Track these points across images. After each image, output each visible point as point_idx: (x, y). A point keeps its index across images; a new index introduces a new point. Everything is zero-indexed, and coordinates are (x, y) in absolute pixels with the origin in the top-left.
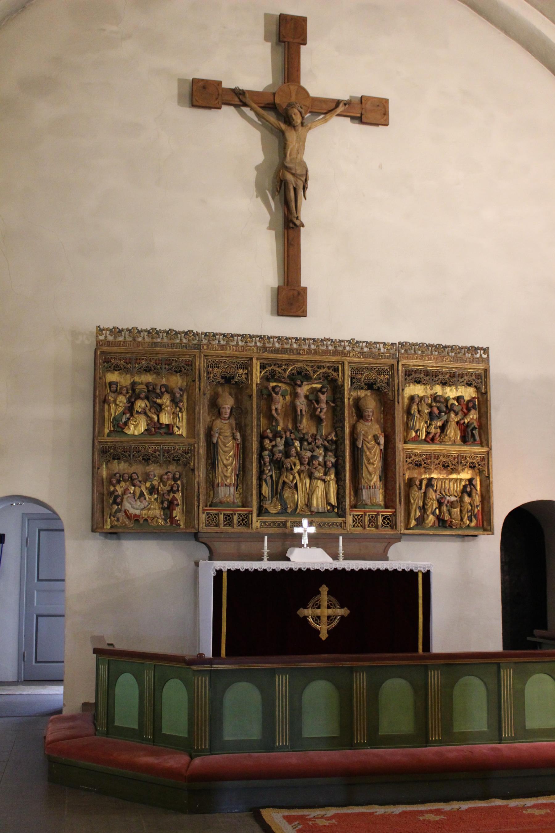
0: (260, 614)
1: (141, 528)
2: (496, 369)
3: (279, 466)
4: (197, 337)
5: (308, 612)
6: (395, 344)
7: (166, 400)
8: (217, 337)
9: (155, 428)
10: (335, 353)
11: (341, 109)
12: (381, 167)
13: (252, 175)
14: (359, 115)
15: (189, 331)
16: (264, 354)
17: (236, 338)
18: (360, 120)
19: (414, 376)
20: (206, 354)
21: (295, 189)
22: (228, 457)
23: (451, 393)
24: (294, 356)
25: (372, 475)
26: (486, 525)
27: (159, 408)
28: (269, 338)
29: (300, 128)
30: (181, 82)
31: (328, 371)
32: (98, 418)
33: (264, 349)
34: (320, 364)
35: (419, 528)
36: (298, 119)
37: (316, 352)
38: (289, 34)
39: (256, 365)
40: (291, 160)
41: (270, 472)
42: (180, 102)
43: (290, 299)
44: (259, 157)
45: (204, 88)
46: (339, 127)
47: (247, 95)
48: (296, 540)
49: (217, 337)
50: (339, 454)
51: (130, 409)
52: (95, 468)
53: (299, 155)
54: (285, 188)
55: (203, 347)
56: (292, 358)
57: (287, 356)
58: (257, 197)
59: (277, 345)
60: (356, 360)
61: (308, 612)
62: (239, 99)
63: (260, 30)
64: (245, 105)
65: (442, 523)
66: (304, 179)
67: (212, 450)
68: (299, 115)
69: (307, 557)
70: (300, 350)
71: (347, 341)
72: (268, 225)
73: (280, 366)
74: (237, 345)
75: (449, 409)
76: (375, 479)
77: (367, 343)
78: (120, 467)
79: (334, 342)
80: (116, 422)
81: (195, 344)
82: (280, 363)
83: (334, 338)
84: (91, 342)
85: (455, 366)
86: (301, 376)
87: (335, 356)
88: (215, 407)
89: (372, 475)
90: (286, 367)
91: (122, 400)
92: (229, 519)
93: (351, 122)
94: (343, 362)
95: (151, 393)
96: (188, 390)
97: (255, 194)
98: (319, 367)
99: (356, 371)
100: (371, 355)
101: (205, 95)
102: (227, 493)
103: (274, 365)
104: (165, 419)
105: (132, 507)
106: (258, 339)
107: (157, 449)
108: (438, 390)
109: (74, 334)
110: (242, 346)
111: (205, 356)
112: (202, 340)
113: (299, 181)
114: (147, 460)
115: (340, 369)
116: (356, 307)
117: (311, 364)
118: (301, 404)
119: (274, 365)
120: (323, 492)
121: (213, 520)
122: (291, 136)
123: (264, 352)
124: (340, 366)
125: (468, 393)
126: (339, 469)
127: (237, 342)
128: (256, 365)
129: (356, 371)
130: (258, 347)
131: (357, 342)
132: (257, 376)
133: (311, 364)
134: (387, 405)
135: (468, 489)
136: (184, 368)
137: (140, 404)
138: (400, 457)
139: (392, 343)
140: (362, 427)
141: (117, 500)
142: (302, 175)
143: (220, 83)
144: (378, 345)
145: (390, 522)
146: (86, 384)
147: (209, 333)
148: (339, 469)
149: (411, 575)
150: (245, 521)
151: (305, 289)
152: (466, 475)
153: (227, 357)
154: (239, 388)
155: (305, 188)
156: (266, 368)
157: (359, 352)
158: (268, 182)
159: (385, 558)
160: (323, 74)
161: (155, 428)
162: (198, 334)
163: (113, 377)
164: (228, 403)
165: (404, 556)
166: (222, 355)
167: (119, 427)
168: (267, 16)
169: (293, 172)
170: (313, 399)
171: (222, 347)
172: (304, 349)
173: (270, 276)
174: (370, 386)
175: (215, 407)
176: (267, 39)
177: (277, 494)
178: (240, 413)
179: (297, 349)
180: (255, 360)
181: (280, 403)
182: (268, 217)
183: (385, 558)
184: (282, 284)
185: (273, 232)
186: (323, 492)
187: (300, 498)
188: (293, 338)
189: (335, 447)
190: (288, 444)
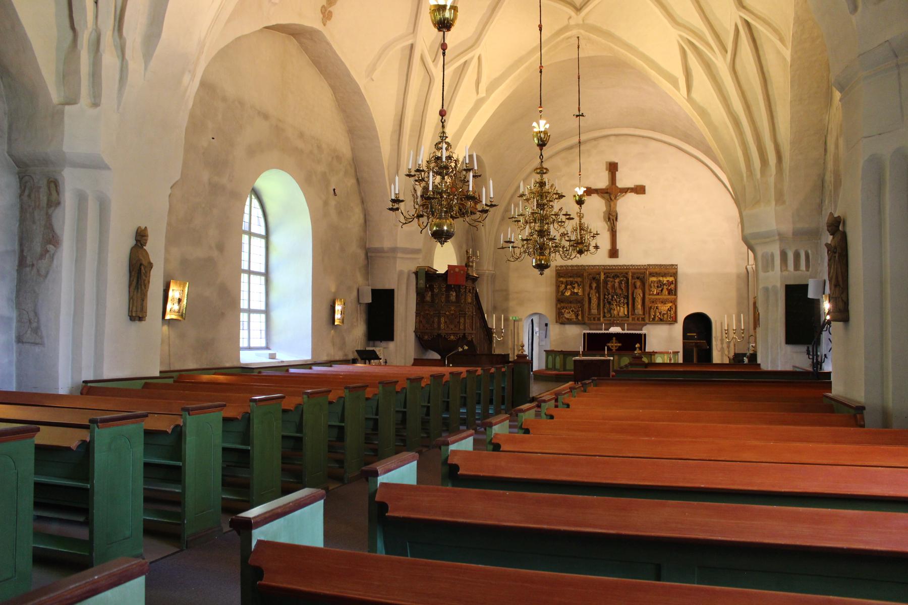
0: (594, 343)
1: (569, 322)
2: (680, 271)
3: (610, 303)
7: (576, 285)
9: (573, 293)
19: (652, 275)
22: (594, 301)
23: (665, 280)
25: (639, 306)
26: (675, 320)
27: (574, 288)
38: (613, 168)
39: (602, 274)
44: (604, 209)
46: (631, 196)
51: (566, 288)
54: (611, 218)
62: (597, 191)
63: (605, 167)
65: (661, 320)
67: (590, 299)
76: (640, 306)
85: (666, 271)
86: (616, 276)
88: (591, 287)
89: (639, 306)
95: (572, 283)
96: (582, 282)
99: (633, 274)
102: (594, 311)
104: (576, 291)
105: (567, 316)
107: (576, 300)
108: (661, 279)
114: (571, 302)
116: (635, 254)
118: (617, 285)
120: (623, 311)
121: (589, 319)
122: (612, 204)
125: (671, 279)
128: (602, 274)
129: (633, 274)
132: (602, 277)
134: (643, 284)
138: (647, 300)
141: (563, 314)
145: (643, 319)
146: (554, 280)
149: (640, 335)
150: (599, 319)
154: (598, 281)
160: (623, 181)
161: (573, 293)
163: (561, 279)
164: (594, 285)
167: (563, 293)
170: (620, 283)
174: (638, 278)
175: (591, 287)
178: (598, 288)
181: (609, 286)
187: (616, 312)
189: (627, 297)
190: (613, 297)
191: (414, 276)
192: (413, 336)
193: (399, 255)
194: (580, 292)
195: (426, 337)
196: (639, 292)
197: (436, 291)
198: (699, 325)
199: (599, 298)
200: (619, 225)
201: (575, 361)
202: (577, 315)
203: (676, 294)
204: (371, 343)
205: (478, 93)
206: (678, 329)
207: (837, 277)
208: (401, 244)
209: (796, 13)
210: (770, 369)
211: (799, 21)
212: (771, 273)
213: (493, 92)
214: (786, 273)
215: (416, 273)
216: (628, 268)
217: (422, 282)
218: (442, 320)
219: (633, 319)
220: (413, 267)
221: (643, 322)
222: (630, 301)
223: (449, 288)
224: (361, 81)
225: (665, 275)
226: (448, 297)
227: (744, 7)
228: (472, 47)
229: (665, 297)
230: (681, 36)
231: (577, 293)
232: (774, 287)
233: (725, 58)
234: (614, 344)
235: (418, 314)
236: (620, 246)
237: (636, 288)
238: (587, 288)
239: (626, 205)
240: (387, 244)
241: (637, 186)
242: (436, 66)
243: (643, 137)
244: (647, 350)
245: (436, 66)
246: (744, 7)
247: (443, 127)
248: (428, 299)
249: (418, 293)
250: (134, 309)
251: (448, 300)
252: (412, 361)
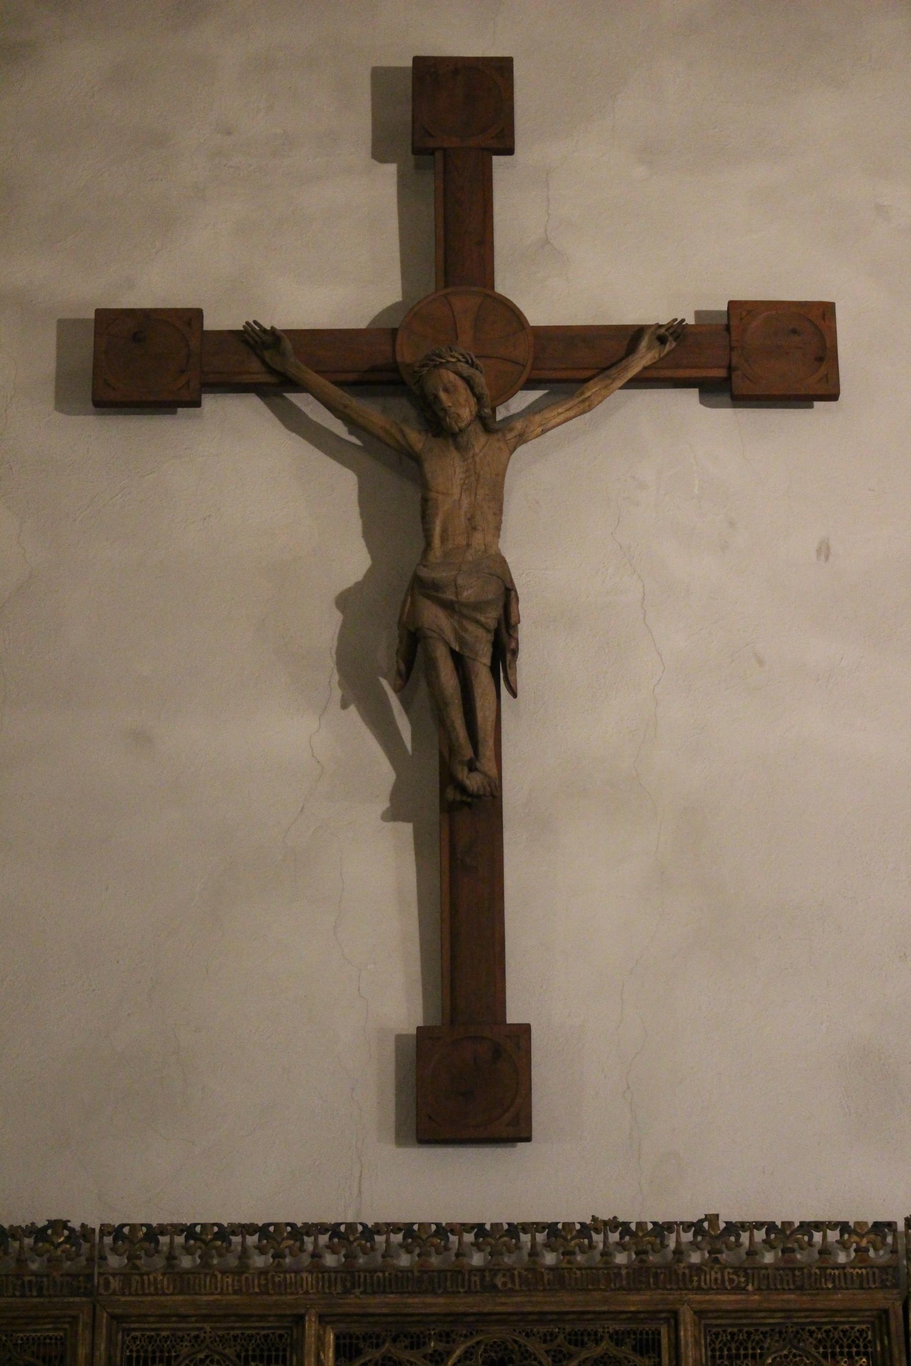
4: (86, 1246)
6: (891, 1225)
8: (164, 1240)
10: (640, 1276)
11: (645, 357)
12: (824, 551)
13: (324, 628)
14: (722, 373)
15: (52, 1224)
16: (351, 1299)
17: (236, 1239)
20: (118, 1311)
21: (459, 661)
24: (470, 1300)
28: (370, 1232)
29: (479, 442)
30: (66, 327)
31: (614, 1351)
33: (349, 1276)
34: (579, 1327)
36: (462, 408)
37: (559, 1278)
38: (452, 126)
40: (446, 554)
42: (65, 401)
43: (467, 1072)
44: (352, 561)
45: (137, 338)
47: (288, 345)
49: (164, 1240)
53: (478, 539)
54: (437, 660)
55: (107, 1284)
56: (461, 1309)
57: (441, 1300)
58: (344, 706)
59: (404, 1260)
60: (726, 1300)
63: (360, 121)
64: (297, 386)
66: (491, 617)
68: (463, 392)
70: (494, 1272)
71: (687, 1226)
72: (384, 804)
73: (416, 1343)
74: (243, 1267)
77: (771, 1227)
79: (633, 1234)
81: (75, 1276)
82: (414, 1330)
83: (631, 1215)
87: (638, 1290)
90: (441, 1346)
93: (702, 402)
94: (675, 1314)
97: (338, 693)
98: (577, 1339)
100: (790, 1275)
101: (147, 364)
103: (394, 1340)
106: (324, 1239)
110: (263, 1272)
111: (113, 1317)
112: (103, 1258)
113: (471, 627)
115: (664, 1341)
117: (543, 1329)
119: (394, 1340)
122: (448, 473)
123: (347, 1291)
124: (664, 1331)
127: (244, 1253)
130: (324, 1270)
131: (733, 1228)
133: (543, 1329)
139: (876, 1225)
142: (478, 606)
143: (198, 314)
144: (817, 1237)
147: (133, 1227)
151: (524, 1030)
153: (205, 1318)
155: (503, 651)
156: (359, 1352)
157: (736, 1270)
158: (384, 648)
160: (580, 245)
162: (86, 1232)
166: (182, 1311)
168: (380, 76)
169: (449, 596)
171: (183, 1281)
172: (510, 1269)
176: (380, 153)
179: (480, 1270)
180: (311, 1327)
182: (384, 773)
184: (436, 1021)
185: (407, 829)
188: (466, 1227)
200: (540, 746)
236: (538, 986)
239: (606, 521)
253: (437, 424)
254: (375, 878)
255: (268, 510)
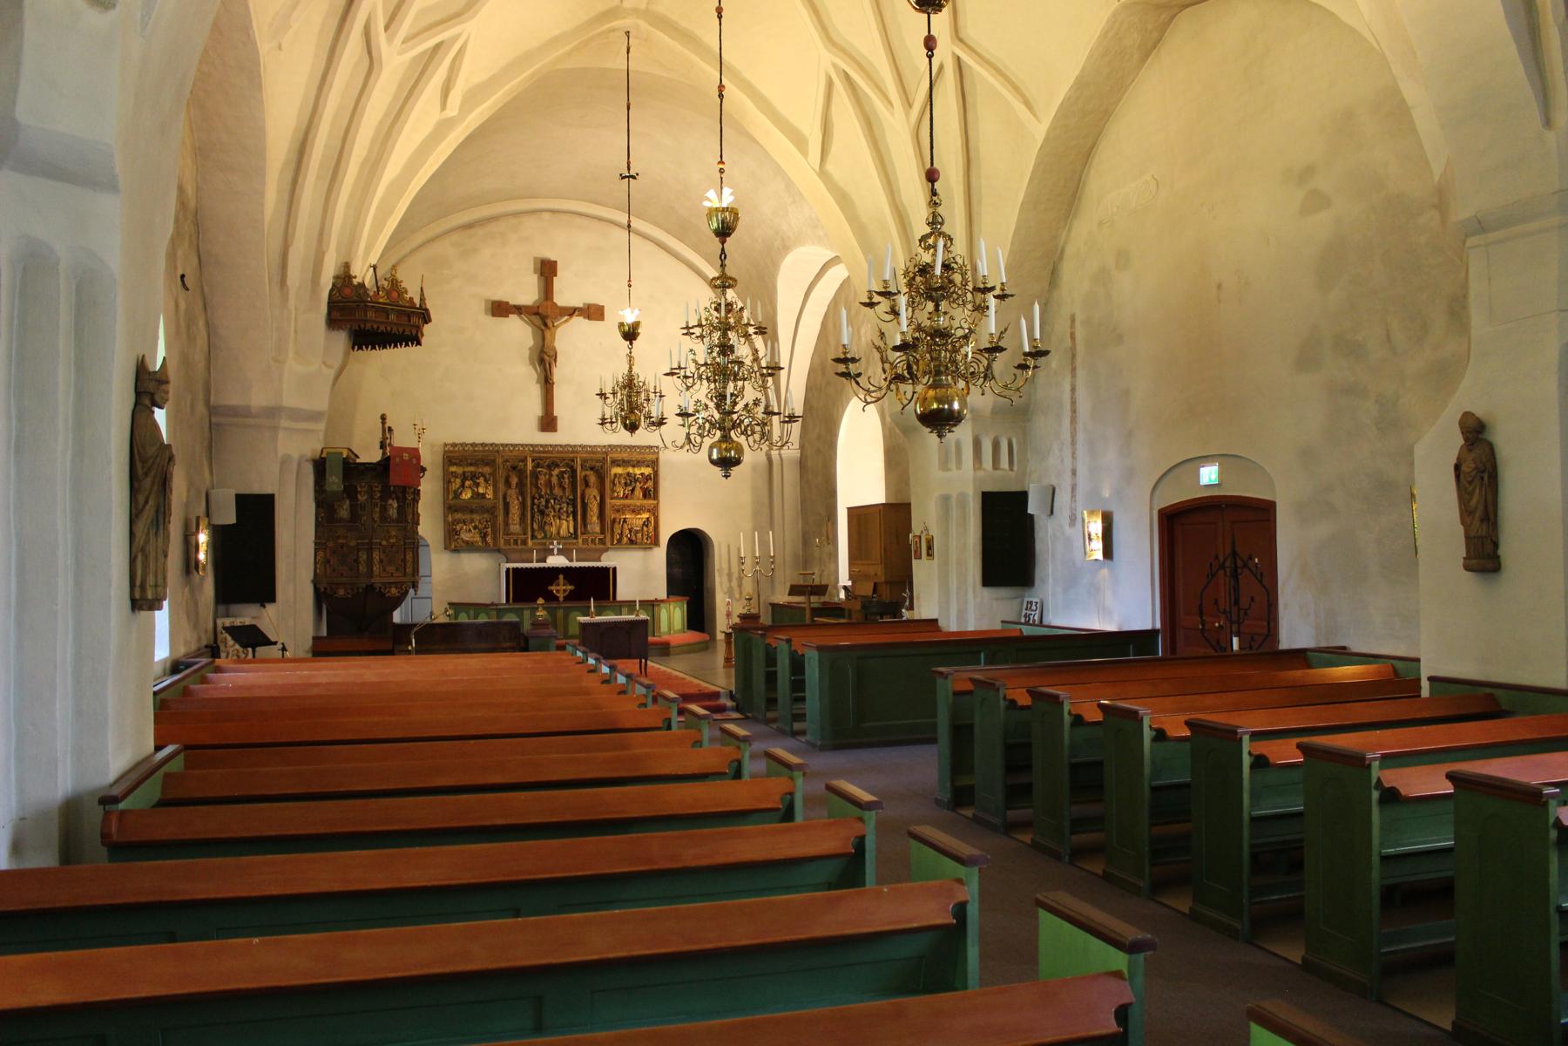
1: (470, 547)
3: (542, 513)
5: (553, 588)
7: (481, 480)
9: (476, 495)
13: (527, 353)
18: (589, 318)
19: (615, 463)
26: (656, 543)
27: (478, 485)
32: (446, 490)
35: (619, 544)
38: (547, 270)
41: (538, 517)
43: (548, 422)
44: (531, 343)
46: (578, 322)
48: (551, 552)
50: (575, 507)
51: (463, 485)
52: (445, 516)
54: (544, 360)
61: (553, 588)
62: (518, 310)
65: (631, 542)
69: (556, 561)
75: (636, 480)
78: (458, 516)
80: (455, 492)
84: (441, 450)
85: (639, 457)
86: (555, 465)
88: (508, 483)
91: (458, 481)
92: (516, 542)
95: (474, 477)
96: (493, 474)
99: (584, 461)
101: (500, 309)
102: (515, 528)
104: (481, 490)
105: (465, 536)
107: (478, 506)
108: (630, 470)
109: (433, 446)
114: (472, 512)
118: (554, 480)
120: (566, 526)
121: (507, 542)
122: (548, 334)
125: (647, 471)
126: (575, 514)
129: (584, 461)
132: (530, 465)
134: (601, 479)
135: (646, 524)
136: (490, 463)
137: (468, 483)
138: (608, 507)
140: (588, 491)
141: (457, 533)
145: (602, 541)
148: (575, 514)
149: (606, 570)
150: (524, 542)
152: (646, 516)
154: (521, 473)
158: (536, 357)
159: (599, 560)
160: (565, 295)
161: (476, 495)
163: (453, 469)
164: (514, 481)
165: (607, 560)
167: (457, 495)
170: (561, 476)
173: (537, 410)
175: (508, 483)
177: (542, 528)
178: (521, 485)
181: (542, 480)
183: (599, 560)
186: (566, 526)
187: (554, 530)
189: (573, 503)
190: (547, 501)
191: (309, 471)
192: (309, 591)
193: (284, 423)
194: (490, 496)
195: (341, 592)
196: (593, 492)
197: (362, 498)
198: (690, 552)
199: (523, 505)
200: (558, 374)
201: (584, 626)
202: (485, 535)
203: (656, 497)
204: (221, 608)
205: (444, 106)
206: (659, 555)
207: (1486, 507)
208: (290, 400)
209: (1083, 71)
210: (953, 628)
211: (1080, 84)
212: (954, 473)
213: (471, 111)
214: (980, 473)
215: (320, 466)
216: (574, 449)
217: (335, 482)
218: (376, 556)
219: (585, 541)
220: (312, 446)
221: (603, 546)
222: (578, 509)
223: (386, 494)
224: (264, 47)
225: (638, 464)
226: (384, 509)
227: (961, 40)
228: (456, 17)
229: (638, 503)
230: (835, 66)
231: (483, 496)
232: (962, 498)
233: (907, 115)
234: (561, 588)
235: (319, 545)
236: (558, 411)
237: (587, 485)
238: (501, 486)
240: (258, 399)
241: (589, 307)
242: (390, 40)
243: (600, 219)
244: (619, 598)
245: (390, 40)
246: (961, 40)
247: (934, 204)
248: (344, 512)
249: (319, 504)
250: (151, 580)
251: (384, 518)
252: (310, 643)
253: (546, 325)
254: (535, 392)
255: (519, 332)
